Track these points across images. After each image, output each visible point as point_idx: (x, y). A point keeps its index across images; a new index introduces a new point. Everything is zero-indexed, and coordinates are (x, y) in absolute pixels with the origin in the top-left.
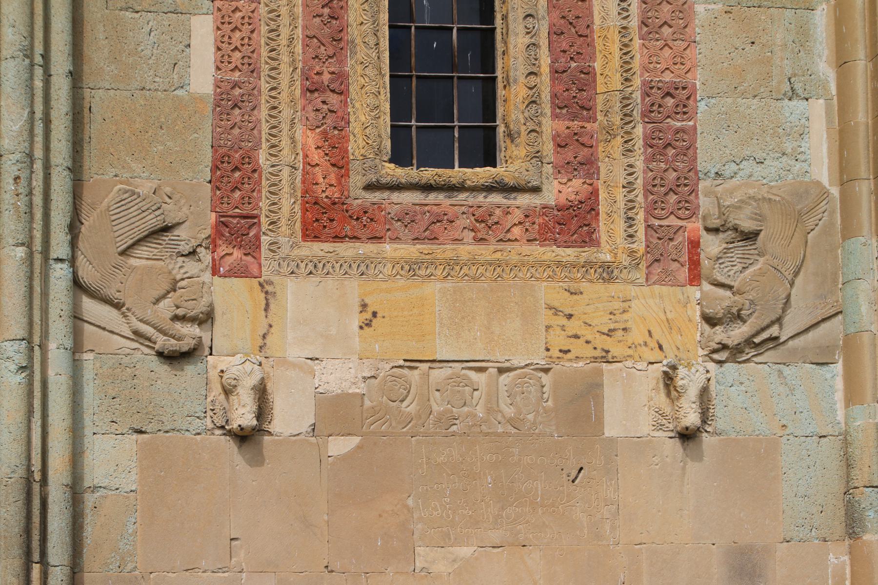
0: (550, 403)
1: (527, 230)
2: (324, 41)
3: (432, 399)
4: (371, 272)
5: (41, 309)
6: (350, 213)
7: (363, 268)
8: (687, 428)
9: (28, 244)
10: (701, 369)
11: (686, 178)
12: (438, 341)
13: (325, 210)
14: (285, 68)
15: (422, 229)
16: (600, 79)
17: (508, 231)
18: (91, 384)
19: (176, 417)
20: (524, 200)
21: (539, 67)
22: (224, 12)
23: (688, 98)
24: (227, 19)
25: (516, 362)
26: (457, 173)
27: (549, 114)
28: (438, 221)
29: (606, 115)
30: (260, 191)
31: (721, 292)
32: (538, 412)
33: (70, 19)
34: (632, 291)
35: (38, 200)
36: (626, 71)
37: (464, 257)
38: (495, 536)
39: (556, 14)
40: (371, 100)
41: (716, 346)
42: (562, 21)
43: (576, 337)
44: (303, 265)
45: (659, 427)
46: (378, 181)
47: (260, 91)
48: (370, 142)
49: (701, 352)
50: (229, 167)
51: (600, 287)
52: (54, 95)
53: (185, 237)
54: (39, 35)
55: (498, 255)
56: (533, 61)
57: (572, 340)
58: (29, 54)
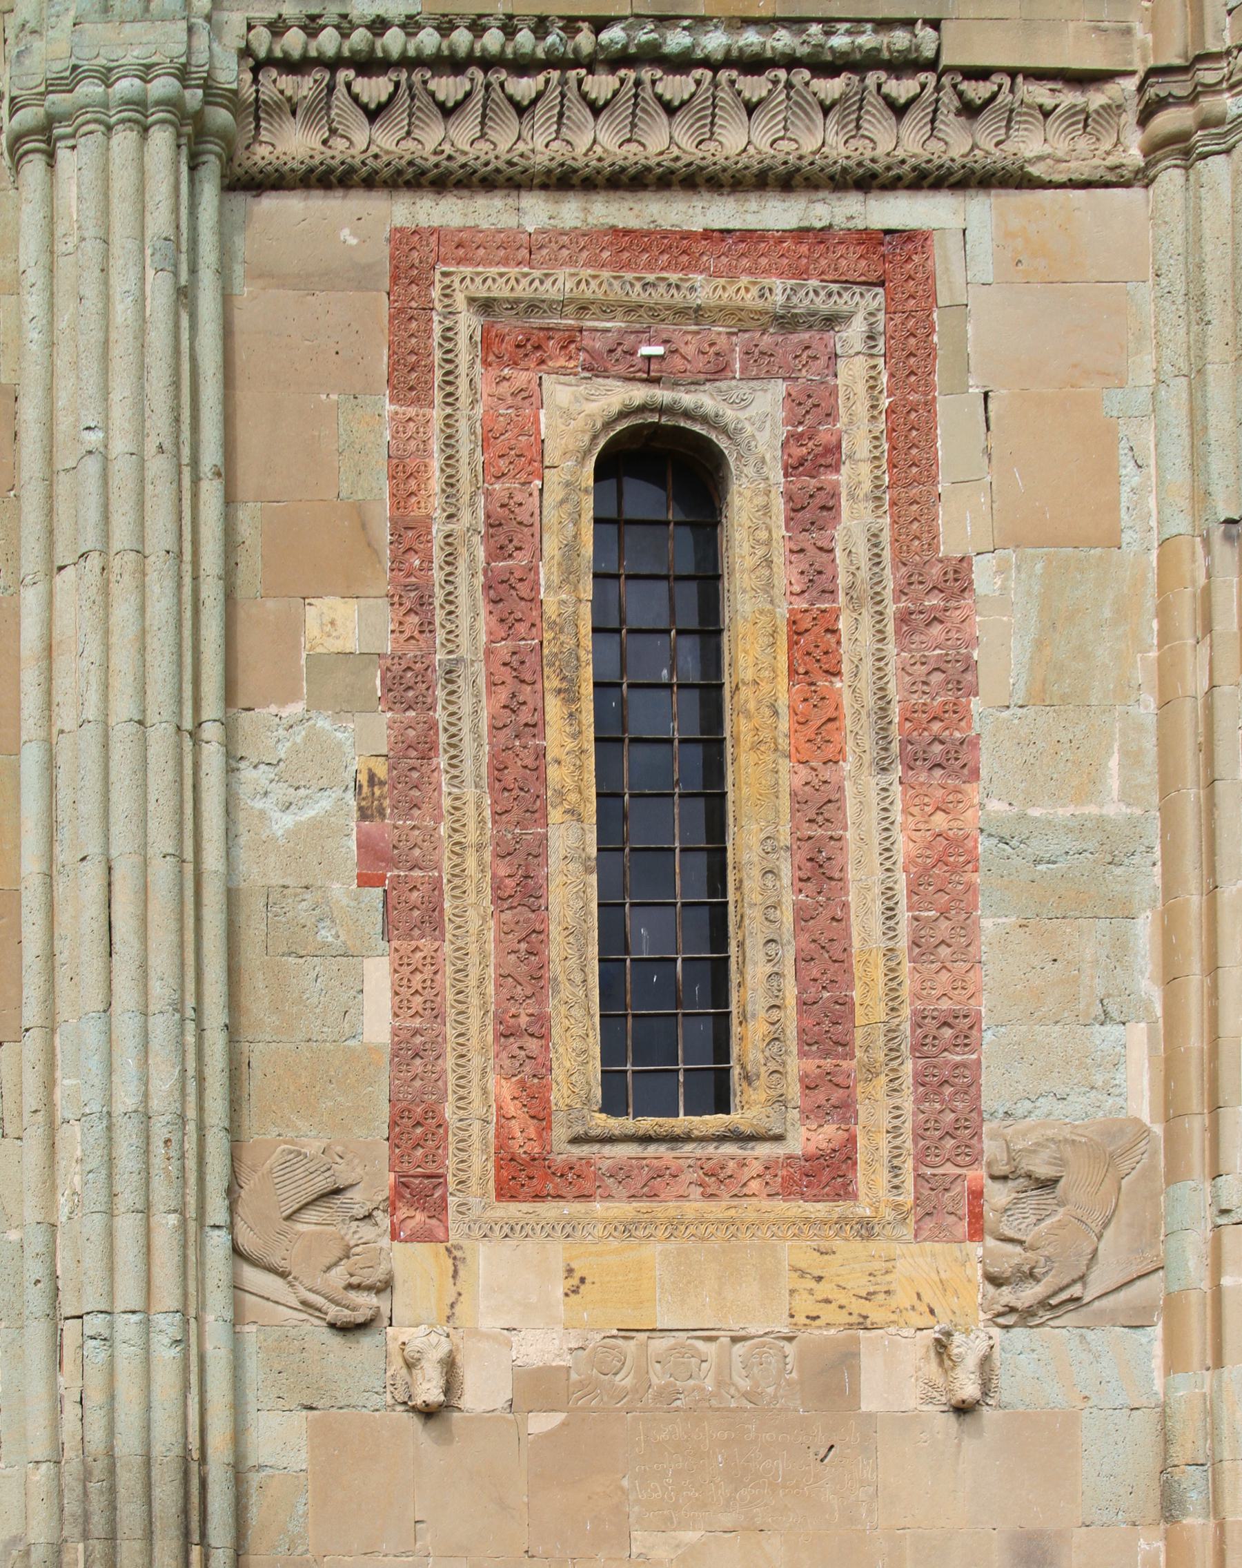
0: (794, 1375)
2: (520, 980)
3: (651, 1371)
4: (578, 1233)
5: (197, 1279)
6: (553, 1169)
7: (568, 1229)
8: (963, 1402)
9: (181, 1211)
10: (982, 1335)
11: (966, 1120)
12: (658, 1308)
13: (523, 1166)
14: (475, 1013)
15: (639, 1186)
16: (859, 1011)
17: (745, 1185)
18: (254, 1358)
19: (350, 1392)
20: (764, 1150)
21: (783, 999)
22: (401, 953)
23: (971, 1028)
24: (405, 960)
25: (752, 1331)
26: (682, 1122)
27: (795, 1052)
28: (659, 1176)
29: (866, 1051)
30: (446, 1148)
31: (1009, 1248)
32: (779, 1385)
33: (225, 968)
35: (191, 1163)
36: (893, 1000)
37: (691, 1215)
38: (727, 1520)
39: (805, 937)
40: (578, 1044)
41: (1002, 1309)
42: (813, 946)
44: (497, 1228)
45: (930, 1400)
46: (586, 1134)
47: (445, 1039)
48: (576, 1090)
49: (982, 1316)
50: (411, 1123)
51: (857, 1246)
52: (207, 1051)
53: (359, 1200)
54: (190, 987)
55: (732, 1212)
56: (776, 993)
57: (822, 1305)
58: (179, 1007)
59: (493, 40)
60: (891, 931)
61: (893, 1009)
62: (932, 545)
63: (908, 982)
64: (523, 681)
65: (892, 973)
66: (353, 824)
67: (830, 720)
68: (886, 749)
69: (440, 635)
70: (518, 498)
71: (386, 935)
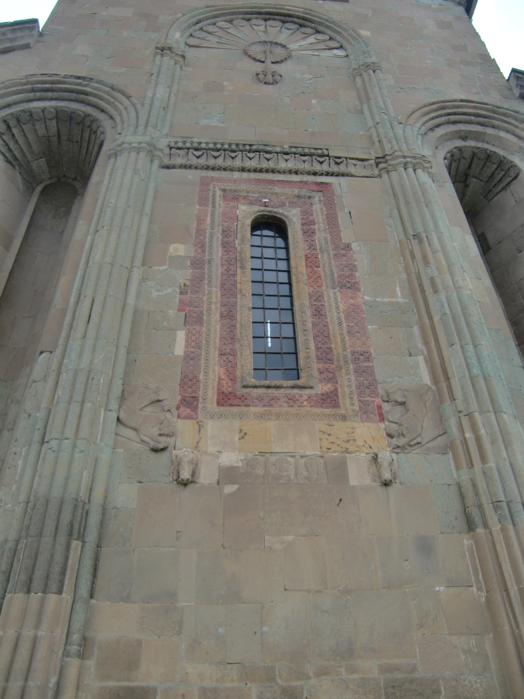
1: (310, 402)
2: (228, 339)
7: (241, 416)
16: (334, 351)
20: (307, 392)
25: (307, 453)
34: (356, 425)
43: (333, 443)
44: (216, 416)
46: (247, 385)
49: (388, 449)
55: (298, 411)
57: (332, 444)
59: (226, 146)
60: (341, 329)
61: (344, 350)
62: (341, 240)
63: (348, 342)
64: (231, 265)
65: (343, 340)
66: (178, 296)
67: (318, 277)
68: (334, 284)
69: (207, 254)
70: (231, 226)
71: (185, 325)
